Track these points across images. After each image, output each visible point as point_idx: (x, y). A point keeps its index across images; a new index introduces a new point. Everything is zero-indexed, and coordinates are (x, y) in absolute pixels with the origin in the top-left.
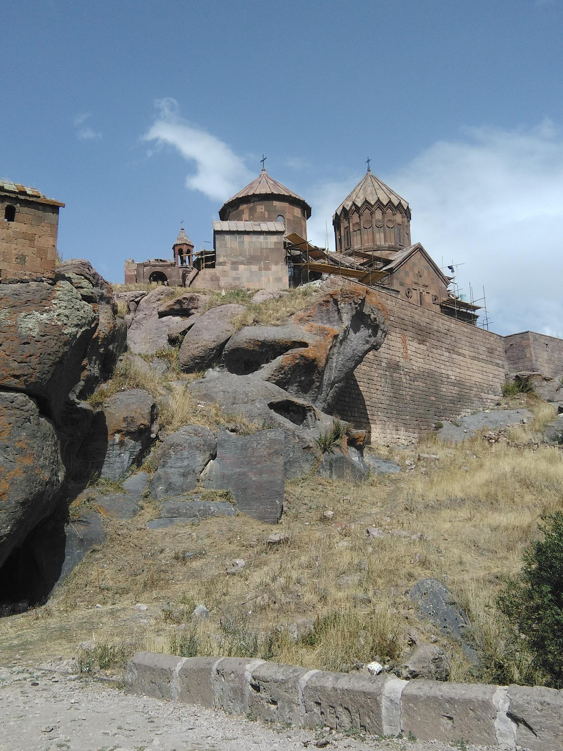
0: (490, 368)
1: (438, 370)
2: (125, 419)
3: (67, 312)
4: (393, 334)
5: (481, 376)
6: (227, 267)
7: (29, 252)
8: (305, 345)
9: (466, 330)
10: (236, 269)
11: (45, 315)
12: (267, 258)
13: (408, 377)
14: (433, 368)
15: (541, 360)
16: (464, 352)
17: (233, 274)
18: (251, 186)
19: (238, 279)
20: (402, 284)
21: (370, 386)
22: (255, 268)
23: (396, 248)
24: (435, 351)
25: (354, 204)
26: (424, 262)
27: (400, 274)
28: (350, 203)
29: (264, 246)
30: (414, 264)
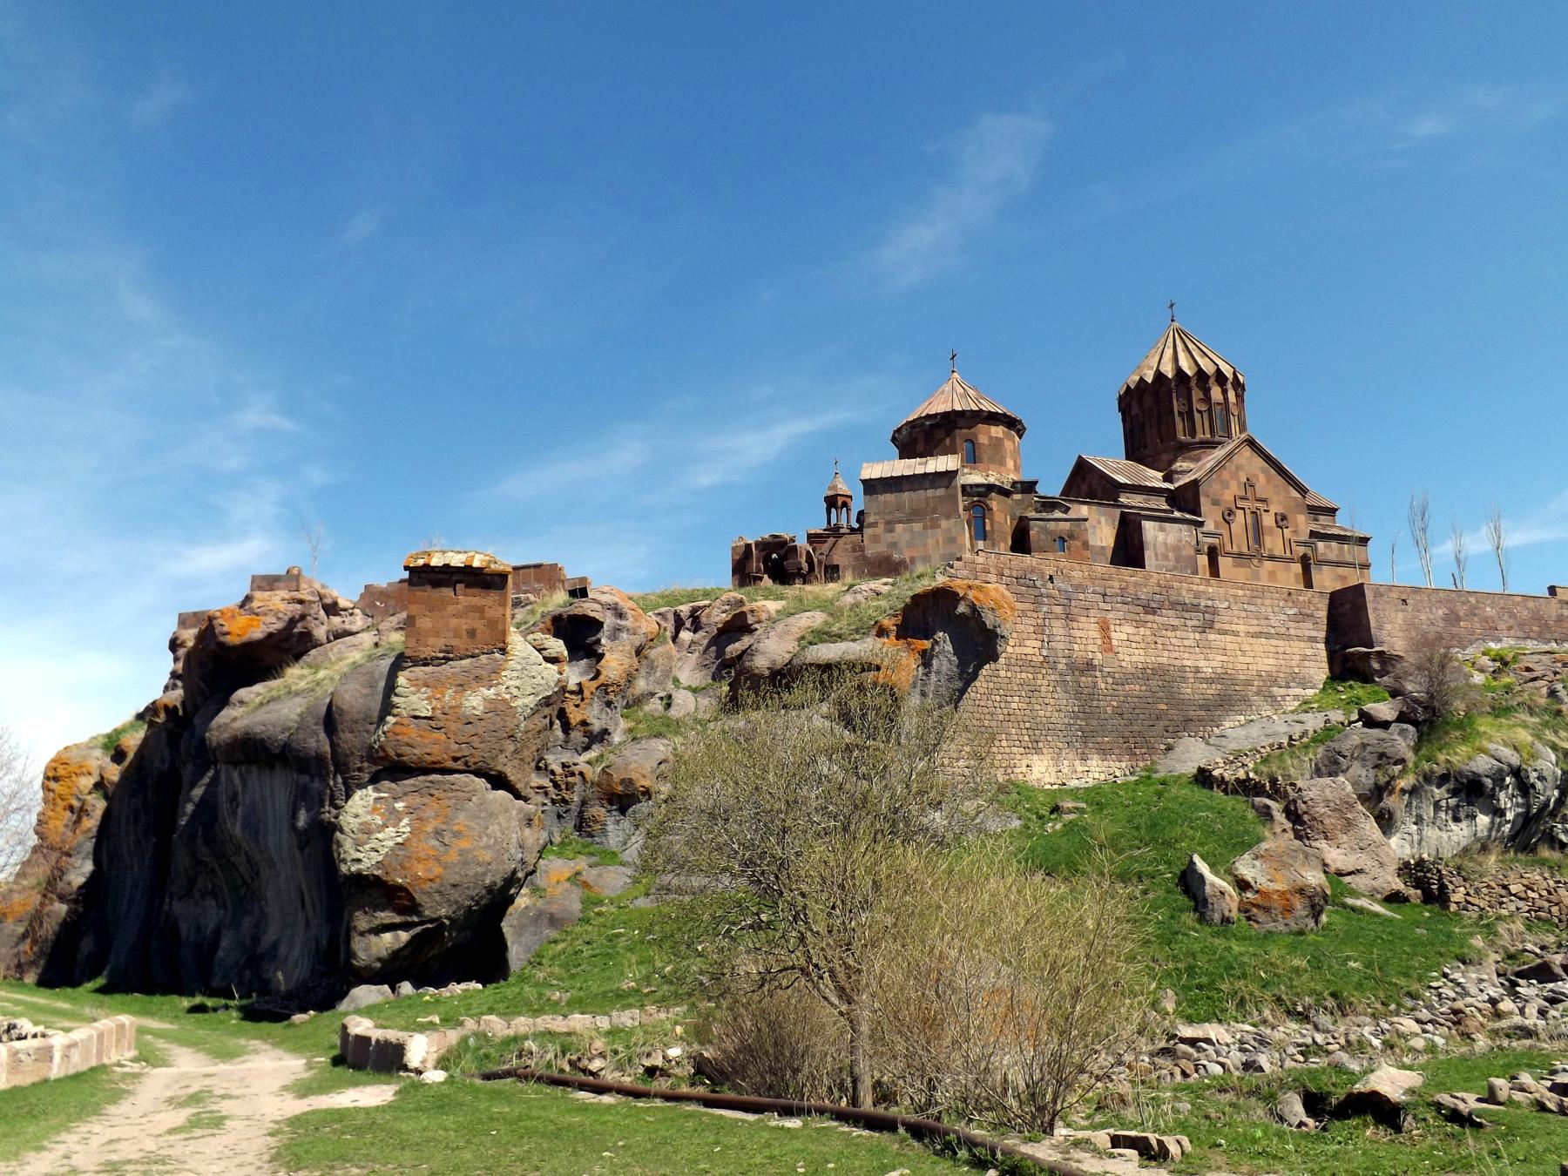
0: (1297, 647)
1: (1177, 663)
2: (623, 781)
3: (517, 683)
4: (1083, 619)
5: (1272, 661)
7: (479, 625)
9: (1240, 593)
10: (892, 531)
11: (493, 690)
12: (935, 511)
13: (1110, 680)
14: (1164, 660)
15: (1388, 627)
16: (1234, 627)
17: (889, 537)
19: (894, 545)
20: (1216, 503)
22: (917, 526)
24: (1169, 634)
25: (1142, 379)
26: (1260, 462)
30: (1238, 468)
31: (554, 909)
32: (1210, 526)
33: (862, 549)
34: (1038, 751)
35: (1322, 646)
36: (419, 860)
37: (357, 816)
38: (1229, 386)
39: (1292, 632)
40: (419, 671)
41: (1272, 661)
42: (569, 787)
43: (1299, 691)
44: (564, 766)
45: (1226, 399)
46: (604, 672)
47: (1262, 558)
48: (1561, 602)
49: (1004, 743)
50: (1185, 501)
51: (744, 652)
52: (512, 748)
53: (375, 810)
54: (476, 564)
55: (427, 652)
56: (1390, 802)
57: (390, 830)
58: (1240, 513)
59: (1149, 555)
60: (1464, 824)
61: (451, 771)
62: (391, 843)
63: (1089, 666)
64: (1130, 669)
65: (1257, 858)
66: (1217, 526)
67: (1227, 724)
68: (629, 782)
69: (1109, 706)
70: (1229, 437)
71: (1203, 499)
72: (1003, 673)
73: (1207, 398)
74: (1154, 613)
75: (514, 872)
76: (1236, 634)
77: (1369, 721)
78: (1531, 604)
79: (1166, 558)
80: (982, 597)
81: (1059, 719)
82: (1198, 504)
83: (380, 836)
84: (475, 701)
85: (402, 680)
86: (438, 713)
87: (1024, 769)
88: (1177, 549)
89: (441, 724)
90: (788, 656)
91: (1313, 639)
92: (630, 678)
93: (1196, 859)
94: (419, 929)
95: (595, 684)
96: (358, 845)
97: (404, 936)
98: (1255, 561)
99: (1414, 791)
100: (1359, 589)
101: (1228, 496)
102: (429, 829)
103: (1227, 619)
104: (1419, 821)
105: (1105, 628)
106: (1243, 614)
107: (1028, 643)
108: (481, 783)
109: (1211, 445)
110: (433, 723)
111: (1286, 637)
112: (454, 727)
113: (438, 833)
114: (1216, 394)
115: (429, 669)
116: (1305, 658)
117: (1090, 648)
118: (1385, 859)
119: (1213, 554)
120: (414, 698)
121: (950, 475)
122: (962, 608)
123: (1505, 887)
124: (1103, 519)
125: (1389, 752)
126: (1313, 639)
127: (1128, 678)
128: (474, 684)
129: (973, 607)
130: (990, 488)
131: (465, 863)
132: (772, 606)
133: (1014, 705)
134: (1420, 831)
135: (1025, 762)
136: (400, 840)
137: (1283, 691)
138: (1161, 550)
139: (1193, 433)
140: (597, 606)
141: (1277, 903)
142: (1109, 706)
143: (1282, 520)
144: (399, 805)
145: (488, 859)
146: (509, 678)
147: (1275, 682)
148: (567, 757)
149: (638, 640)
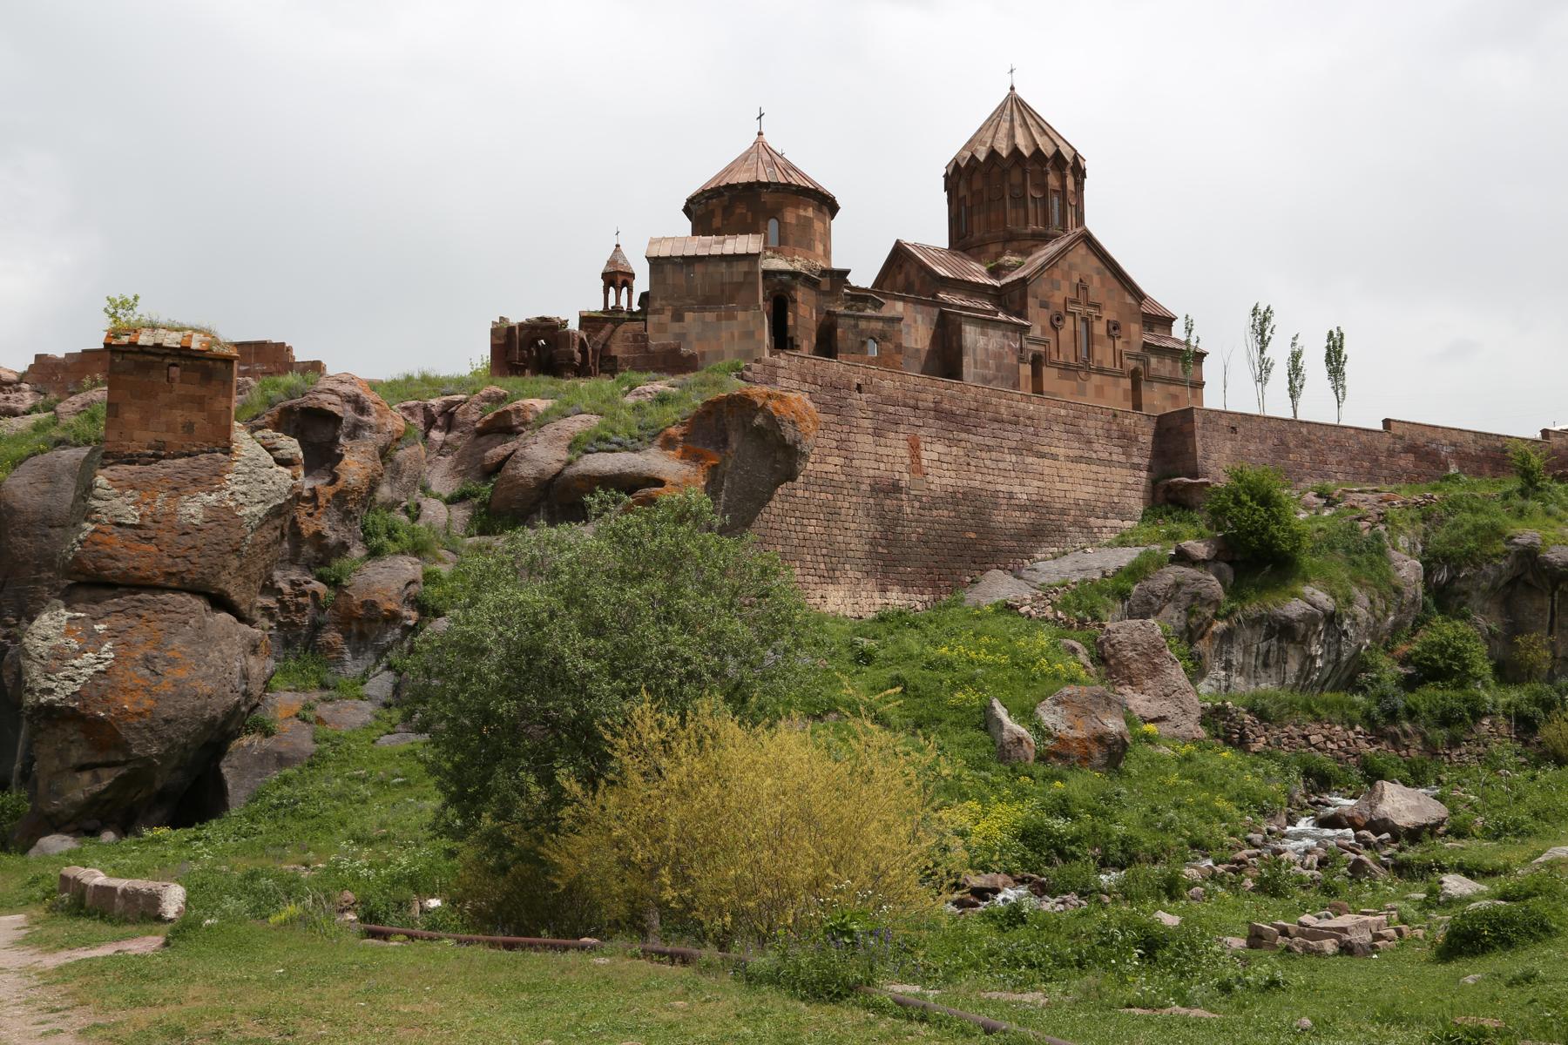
1: (990, 487)
2: (364, 604)
3: (244, 488)
5: (1091, 489)
6: (666, 317)
8: (660, 483)
9: (1063, 412)
10: (678, 317)
13: (917, 504)
16: (1054, 450)
17: (676, 327)
18: (729, 170)
19: (682, 336)
20: (1044, 305)
21: (832, 524)
22: (710, 316)
23: (1046, 236)
24: (984, 455)
25: (973, 156)
26: (1094, 262)
27: (1040, 288)
28: (968, 154)
29: (726, 279)
30: (1071, 267)
31: (283, 748)
32: (1036, 332)
33: (646, 339)
34: (834, 581)
35: (1144, 474)
36: (125, 691)
37: (46, 639)
38: (1068, 172)
39: (1115, 457)
40: (123, 470)
41: (1091, 489)
42: (300, 609)
43: (1117, 522)
44: (293, 583)
45: (1064, 186)
46: (343, 477)
47: (1089, 371)
48: (1394, 436)
49: (798, 571)
50: (1012, 298)
51: (507, 458)
52: (236, 563)
53: (68, 632)
54: (195, 345)
55: (133, 447)
56: (1201, 646)
57: (89, 657)
58: (1069, 320)
59: (967, 361)
60: (1273, 672)
61: (164, 589)
62: (91, 671)
63: (895, 488)
64: (939, 493)
65: (1058, 703)
66: (1043, 333)
67: (1039, 556)
68: (371, 605)
69: (913, 532)
70: (1065, 230)
71: (1030, 301)
72: (800, 493)
73: (1043, 186)
74: (968, 432)
75: (238, 704)
76: (1054, 457)
77: (1182, 557)
78: (1363, 438)
79: (986, 366)
80: (782, 408)
81: (859, 547)
82: (1025, 306)
83: (76, 662)
84: (193, 508)
85: (101, 480)
86: (148, 521)
87: (818, 600)
88: (998, 356)
89: (151, 534)
90: (559, 466)
91: (1136, 467)
92: (373, 485)
93: (996, 703)
94: (123, 771)
95: (331, 490)
96: (48, 673)
97: (107, 778)
98: (1082, 374)
99: (1228, 636)
100: (1187, 414)
101: (1058, 298)
102: (138, 656)
103: (1047, 441)
104: (1228, 666)
105: (914, 447)
106: (1064, 436)
107: (829, 459)
108: (199, 604)
109: (1043, 239)
110: (142, 533)
111: (1109, 463)
112: (167, 537)
113: (148, 661)
114: (1053, 181)
115: (136, 468)
116: (1126, 486)
117: (897, 467)
118: (1189, 708)
119: (1037, 362)
120: (116, 502)
121: (751, 258)
122: (759, 420)
123: (1305, 737)
124: (919, 318)
125: (1205, 592)
126: (1136, 467)
127: (935, 503)
128: (191, 488)
129: (770, 417)
130: (795, 275)
131: (181, 695)
132: (541, 405)
133: (811, 529)
134: (1228, 677)
135: (819, 593)
136: (101, 667)
137: (1100, 522)
138: (980, 356)
139: (1027, 223)
140: (334, 398)
141: (1076, 751)
142: (913, 532)
143: (1114, 328)
144: (100, 627)
145: (207, 690)
146: (234, 483)
147: (1092, 512)
148: (295, 574)
149: (381, 440)
